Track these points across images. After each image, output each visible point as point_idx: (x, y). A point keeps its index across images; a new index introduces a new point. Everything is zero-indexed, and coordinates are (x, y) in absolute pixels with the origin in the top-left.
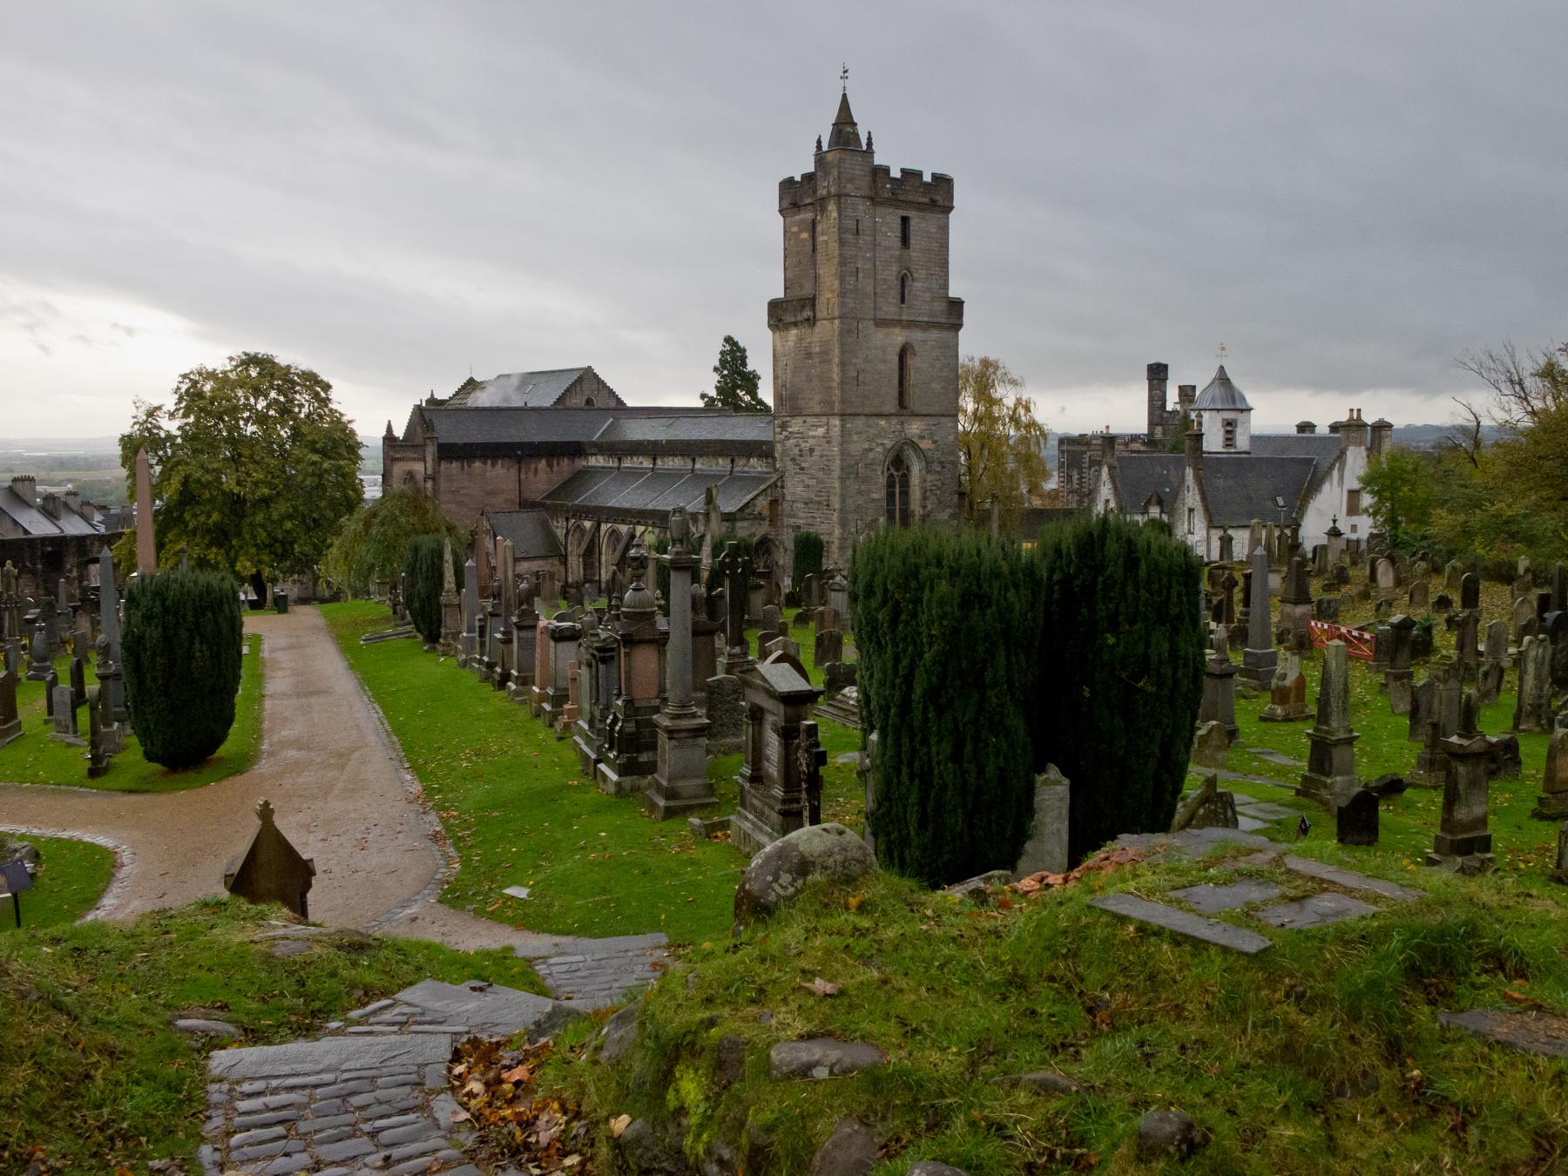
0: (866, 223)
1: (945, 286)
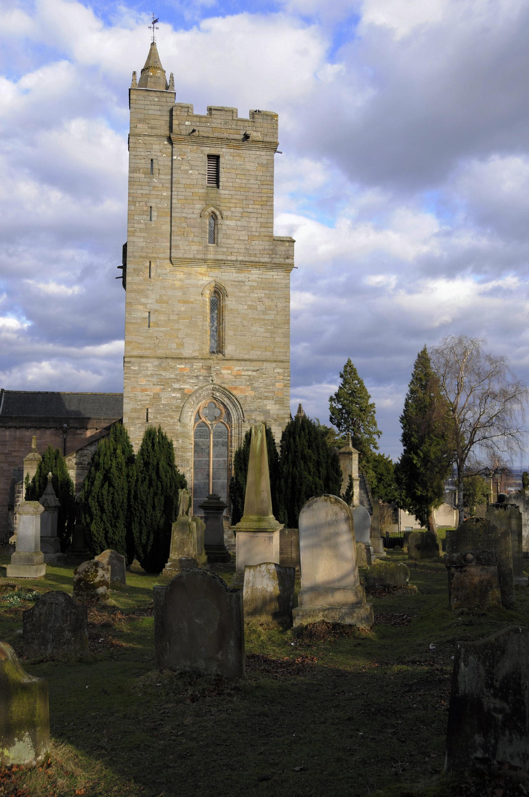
0: (163, 161)
1: (269, 224)
